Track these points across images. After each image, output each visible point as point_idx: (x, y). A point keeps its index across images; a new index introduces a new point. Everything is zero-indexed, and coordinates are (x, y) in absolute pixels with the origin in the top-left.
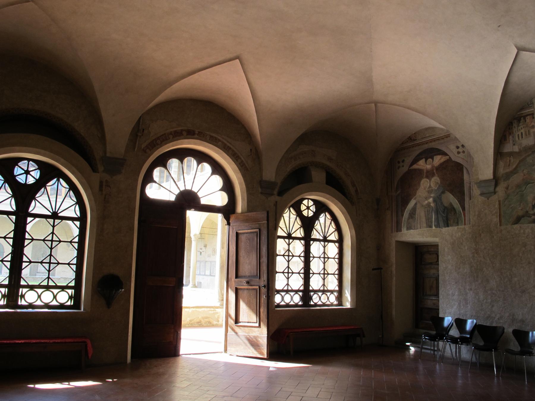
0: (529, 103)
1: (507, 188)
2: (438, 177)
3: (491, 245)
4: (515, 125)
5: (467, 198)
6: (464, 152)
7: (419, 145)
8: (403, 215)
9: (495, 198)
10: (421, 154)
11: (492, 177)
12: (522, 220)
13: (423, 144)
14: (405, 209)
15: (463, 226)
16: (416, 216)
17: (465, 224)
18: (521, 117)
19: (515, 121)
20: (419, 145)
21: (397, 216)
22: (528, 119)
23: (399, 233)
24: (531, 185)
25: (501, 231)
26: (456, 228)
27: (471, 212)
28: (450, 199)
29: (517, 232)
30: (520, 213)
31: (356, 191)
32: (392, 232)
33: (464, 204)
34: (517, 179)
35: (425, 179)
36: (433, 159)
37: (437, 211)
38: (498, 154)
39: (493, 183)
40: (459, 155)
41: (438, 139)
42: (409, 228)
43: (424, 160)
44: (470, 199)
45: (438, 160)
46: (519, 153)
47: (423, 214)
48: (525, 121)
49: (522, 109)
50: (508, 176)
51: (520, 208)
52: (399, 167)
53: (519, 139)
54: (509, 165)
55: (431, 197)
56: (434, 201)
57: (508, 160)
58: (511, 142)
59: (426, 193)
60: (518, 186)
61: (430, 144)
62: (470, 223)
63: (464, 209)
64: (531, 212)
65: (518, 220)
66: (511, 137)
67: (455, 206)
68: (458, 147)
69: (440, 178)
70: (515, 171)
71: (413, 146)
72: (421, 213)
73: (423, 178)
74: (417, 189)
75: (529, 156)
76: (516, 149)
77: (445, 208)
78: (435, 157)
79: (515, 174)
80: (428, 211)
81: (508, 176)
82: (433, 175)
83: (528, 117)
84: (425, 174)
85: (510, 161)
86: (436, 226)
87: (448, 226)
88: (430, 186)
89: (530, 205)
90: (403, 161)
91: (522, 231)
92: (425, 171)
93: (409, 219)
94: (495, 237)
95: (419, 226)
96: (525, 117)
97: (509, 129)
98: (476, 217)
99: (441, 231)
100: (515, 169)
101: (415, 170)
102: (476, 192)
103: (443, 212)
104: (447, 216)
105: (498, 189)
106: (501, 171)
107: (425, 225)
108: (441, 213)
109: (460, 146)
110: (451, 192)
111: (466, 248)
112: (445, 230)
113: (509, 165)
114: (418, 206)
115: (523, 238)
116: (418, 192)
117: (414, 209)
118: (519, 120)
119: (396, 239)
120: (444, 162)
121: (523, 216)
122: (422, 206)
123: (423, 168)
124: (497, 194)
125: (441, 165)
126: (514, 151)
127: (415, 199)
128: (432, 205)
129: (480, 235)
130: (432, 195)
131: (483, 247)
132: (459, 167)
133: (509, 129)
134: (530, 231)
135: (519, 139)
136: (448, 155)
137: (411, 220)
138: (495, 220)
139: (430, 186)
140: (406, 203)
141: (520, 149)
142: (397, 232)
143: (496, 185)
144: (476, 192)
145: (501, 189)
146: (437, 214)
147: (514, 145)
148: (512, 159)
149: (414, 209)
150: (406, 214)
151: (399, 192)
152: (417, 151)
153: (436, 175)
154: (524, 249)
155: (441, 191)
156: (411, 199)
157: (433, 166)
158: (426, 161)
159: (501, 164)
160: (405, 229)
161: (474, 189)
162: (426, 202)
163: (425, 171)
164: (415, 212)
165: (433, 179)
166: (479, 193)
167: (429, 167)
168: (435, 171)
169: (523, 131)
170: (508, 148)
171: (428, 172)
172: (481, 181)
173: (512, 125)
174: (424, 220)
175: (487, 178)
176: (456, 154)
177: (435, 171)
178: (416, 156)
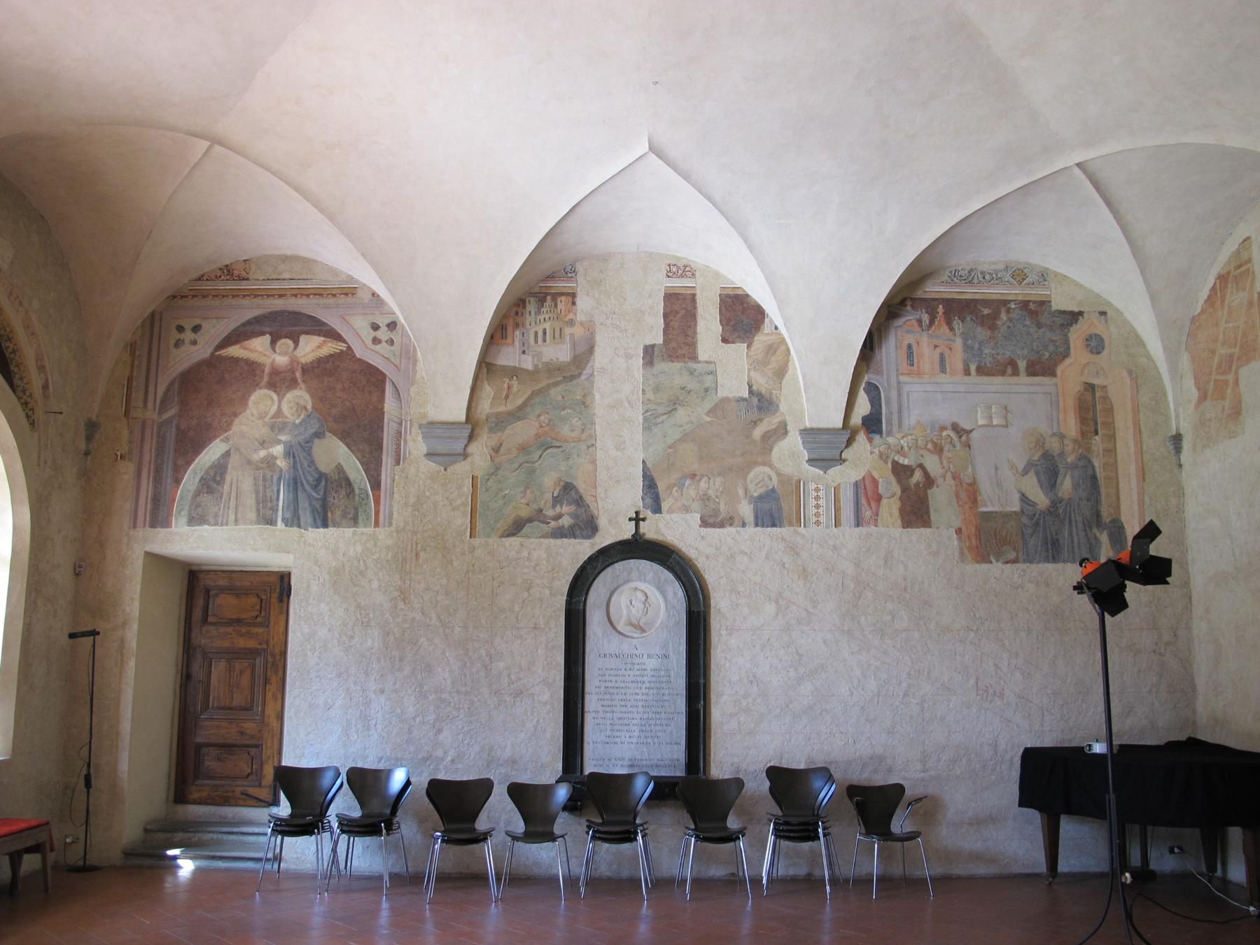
0: (568, 269)
1: (496, 450)
2: (308, 390)
3: (444, 581)
4: (531, 307)
5: (387, 460)
6: (391, 342)
7: (255, 294)
8: (178, 481)
9: (462, 468)
10: (258, 320)
11: (463, 418)
12: (526, 530)
13: (269, 295)
14: (189, 463)
15: (371, 530)
16: (226, 487)
17: (377, 524)
18: (547, 294)
19: (532, 299)
20: (255, 294)
21: (158, 481)
22: (562, 303)
23: (161, 532)
24: (554, 450)
25: (473, 549)
26: (349, 531)
27: (396, 496)
28: (336, 454)
29: (513, 554)
30: (524, 513)
31: (45, 387)
32: (135, 527)
33: (379, 475)
34: (523, 431)
35: (266, 391)
36: (296, 343)
37: (295, 483)
38: (486, 367)
39: (466, 433)
40: (377, 347)
41: (319, 293)
42: (197, 519)
43: (267, 338)
44: (398, 463)
45: (310, 348)
46: (533, 374)
47: (247, 485)
48: (556, 306)
49: (551, 277)
50: (500, 422)
51: (523, 501)
52: (178, 344)
53: (536, 341)
54: (507, 397)
55: (279, 442)
56: (289, 453)
58: (517, 344)
59: (263, 427)
60: (523, 449)
61: (292, 301)
62: (390, 524)
63: (376, 485)
64: (550, 513)
65: (516, 528)
66: (517, 333)
67: (352, 475)
68: (375, 327)
69: (312, 396)
70: (518, 414)
71: (236, 294)
72: (241, 481)
73: (257, 386)
74: (235, 415)
75: (556, 384)
76: (528, 363)
77: (322, 476)
79: (519, 419)
80: (265, 479)
81: (500, 422)
82: (293, 384)
83: (563, 298)
84: (266, 379)
85: (509, 387)
86: (287, 523)
87: (325, 525)
88: (279, 413)
89: (548, 496)
90: (196, 329)
91: (525, 554)
92: (267, 370)
93: (198, 493)
94: (455, 564)
95: (232, 517)
96: (555, 296)
97: (517, 313)
98: (410, 509)
99: (302, 536)
100: (520, 408)
101: (237, 360)
102: (416, 445)
103: (315, 487)
104: (324, 500)
105: (472, 448)
106: (485, 407)
107: (252, 515)
108: (308, 488)
109: (383, 321)
110: (344, 436)
111: (375, 585)
112: (316, 535)
113: (507, 397)
114: (234, 460)
115: (526, 570)
116: (236, 422)
117: (218, 471)
118: (542, 301)
119: (148, 549)
120: (331, 355)
122: (249, 462)
123: (262, 360)
124: (469, 459)
125: (320, 361)
126: (524, 366)
127: (227, 440)
128: (281, 463)
129: (417, 555)
130: (283, 438)
131: (423, 585)
132: (374, 379)
133: (517, 313)
134: (545, 556)
135: (536, 341)
136: (344, 341)
137: (205, 498)
138: (459, 521)
139: (279, 413)
140: (191, 444)
141: (536, 366)
142: (153, 526)
143: (471, 438)
144: (416, 445)
145: (480, 451)
146: (296, 490)
147: (524, 352)
148: (515, 383)
149: (218, 471)
150: (191, 479)
151: (172, 412)
152: (250, 310)
153: (303, 386)
154: (526, 594)
155: (312, 431)
156: (211, 440)
157: (293, 361)
158: (273, 342)
159: (488, 391)
160: (184, 520)
161: (409, 438)
162: (262, 453)
163: (267, 370)
164: (223, 478)
165: (290, 396)
166: (425, 450)
167: (281, 360)
168: (298, 374)
169: (547, 326)
170: (508, 356)
171: (275, 372)
172: (432, 423)
173: (524, 307)
174: (250, 501)
175: (451, 418)
176: (369, 342)
177: (298, 374)
178: (243, 325)
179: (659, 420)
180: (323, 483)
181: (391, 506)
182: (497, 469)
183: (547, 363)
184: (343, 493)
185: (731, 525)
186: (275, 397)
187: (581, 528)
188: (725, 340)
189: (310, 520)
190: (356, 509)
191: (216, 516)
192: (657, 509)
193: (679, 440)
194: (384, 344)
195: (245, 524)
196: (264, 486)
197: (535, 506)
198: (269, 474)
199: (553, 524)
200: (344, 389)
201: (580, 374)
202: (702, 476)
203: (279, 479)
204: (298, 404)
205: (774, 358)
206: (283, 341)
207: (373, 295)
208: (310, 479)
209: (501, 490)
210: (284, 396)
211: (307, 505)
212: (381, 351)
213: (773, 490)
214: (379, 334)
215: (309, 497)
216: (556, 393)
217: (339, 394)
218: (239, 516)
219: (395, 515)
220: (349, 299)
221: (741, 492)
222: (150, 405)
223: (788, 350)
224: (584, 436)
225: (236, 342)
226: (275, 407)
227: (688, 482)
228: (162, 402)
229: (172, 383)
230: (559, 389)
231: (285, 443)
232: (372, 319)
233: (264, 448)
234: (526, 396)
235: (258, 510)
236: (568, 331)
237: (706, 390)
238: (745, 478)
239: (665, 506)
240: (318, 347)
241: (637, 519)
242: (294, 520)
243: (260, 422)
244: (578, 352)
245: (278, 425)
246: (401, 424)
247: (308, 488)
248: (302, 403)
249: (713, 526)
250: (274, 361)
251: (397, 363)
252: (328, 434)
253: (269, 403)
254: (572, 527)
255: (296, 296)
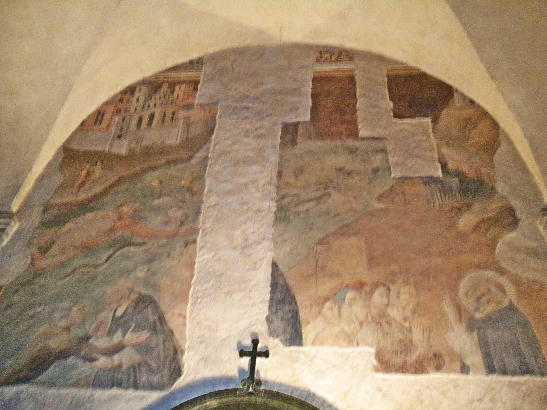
48: (172, 91)
51: (63, 323)
54: (82, 184)
57: (84, 173)
60: (88, 248)
79: (91, 210)
85: (89, 173)
113: (82, 184)
121: (63, 355)
148: (98, 171)
179: (302, 208)
182: (37, 275)
183: (147, 147)
185: (438, 368)
187: (151, 371)
188: (397, 115)
192: (295, 338)
193: (334, 234)
197: (77, 332)
199: (102, 362)
201: (190, 158)
202: (375, 286)
205: (474, 133)
209: (32, 306)
213: (511, 307)
216: (152, 179)
221: (449, 310)
223: (495, 125)
224: (182, 230)
227: (350, 294)
230: (156, 173)
234: (109, 183)
236: (182, 114)
237: (376, 171)
238: (454, 289)
239: (308, 332)
241: (253, 352)
244: (191, 136)
249: (402, 369)
254: (135, 368)
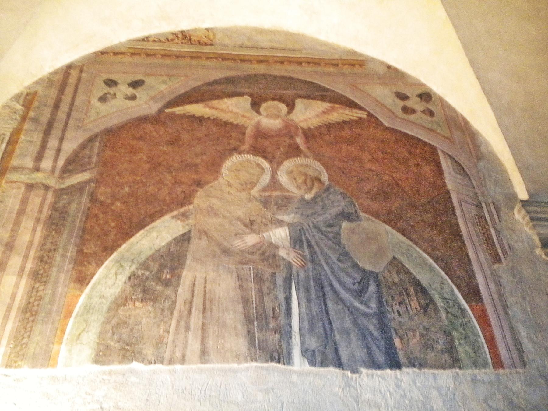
6: (431, 113)
16: (183, 292)
33: (472, 276)
35: (251, 158)
36: (291, 106)
40: (412, 117)
43: (245, 102)
55: (280, 223)
77: (366, 277)
78: (300, 104)
80: (259, 279)
82: (294, 151)
86: (313, 358)
88: (274, 184)
95: (194, 345)
103: (359, 294)
107: (241, 344)
108: (344, 294)
122: (226, 252)
123: (241, 121)
127: (185, 216)
130: (287, 218)
136: (361, 108)
139: (274, 184)
158: (256, 105)
162: (251, 239)
165: (288, 164)
177: (299, 140)
180: (372, 288)
181: (512, 328)
184: (414, 304)
186: (265, 164)
189: (360, 353)
190: (447, 333)
191: (159, 343)
194: (419, 114)
195: (225, 360)
196: (260, 292)
198: (268, 271)
200: (374, 160)
203: (288, 280)
204: (305, 175)
206: (270, 103)
207: (389, 67)
208: (347, 280)
210: (280, 163)
211: (348, 324)
212: (419, 121)
214: (409, 104)
215: (352, 312)
217: (369, 166)
218: (210, 343)
219: (527, 346)
220: (357, 70)
222: (46, 164)
225: (197, 101)
226: (266, 178)
228: (69, 162)
229: (91, 140)
231: (291, 225)
232: (395, 89)
233: (253, 231)
235: (250, 334)
240: (324, 112)
242: (326, 355)
243: (244, 195)
245: (274, 200)
246: (479, 205)
247: (344, 294)
248: (311, 173)
250: (259, 123)
251: (447, 134)
252: (363, 215)
253: (257, 171)
255: (282, 63)
